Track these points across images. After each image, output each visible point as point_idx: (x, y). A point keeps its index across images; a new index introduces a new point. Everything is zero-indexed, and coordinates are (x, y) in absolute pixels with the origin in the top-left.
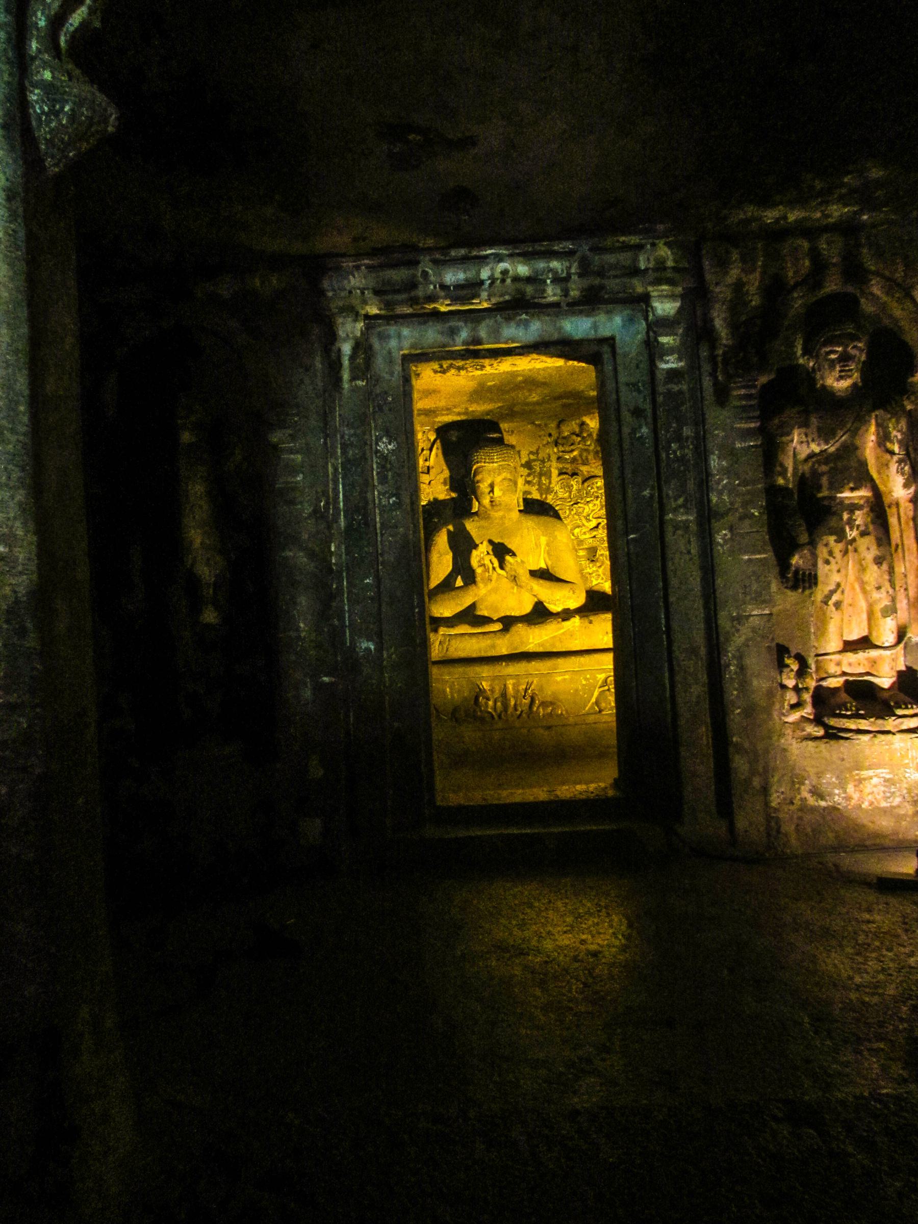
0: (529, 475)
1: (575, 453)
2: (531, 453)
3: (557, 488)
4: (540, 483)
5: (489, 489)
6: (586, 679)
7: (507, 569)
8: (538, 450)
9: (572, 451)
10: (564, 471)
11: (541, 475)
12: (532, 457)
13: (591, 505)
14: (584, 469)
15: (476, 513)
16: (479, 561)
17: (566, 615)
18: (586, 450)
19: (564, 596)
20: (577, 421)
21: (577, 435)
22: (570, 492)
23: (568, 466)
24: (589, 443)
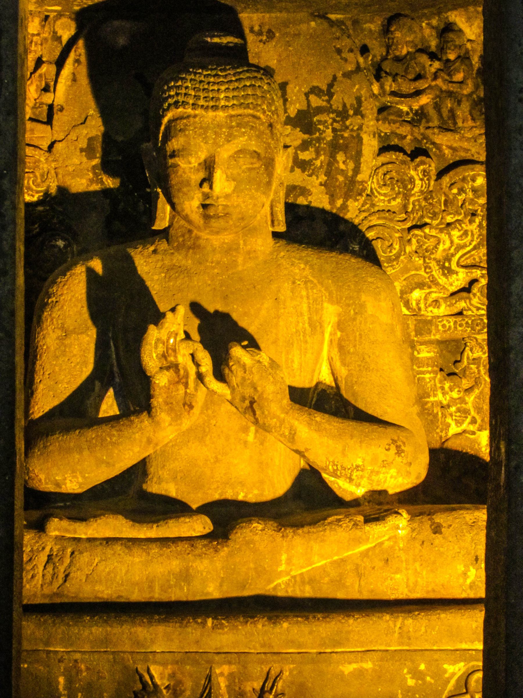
0: (304, 146)
1: (424, 100)
2: (315, 91)
3: (372, 184)
4: (330, 170)
5: (201, 175)
6: (417, 674)
7: (234, 381)
8: (330, 86)
9: (418, 93)
10: (395, 141)
11: (335, 147)
12: (316, 101)
13: (455, 233)
14: (444, 140)
15: (165, 234)
16: (164, 356)
17: (377, 506)
18: (450, 94)
19: (374, 460)
20: (434, 22)
21: (433, 56)
24: (459, 77)
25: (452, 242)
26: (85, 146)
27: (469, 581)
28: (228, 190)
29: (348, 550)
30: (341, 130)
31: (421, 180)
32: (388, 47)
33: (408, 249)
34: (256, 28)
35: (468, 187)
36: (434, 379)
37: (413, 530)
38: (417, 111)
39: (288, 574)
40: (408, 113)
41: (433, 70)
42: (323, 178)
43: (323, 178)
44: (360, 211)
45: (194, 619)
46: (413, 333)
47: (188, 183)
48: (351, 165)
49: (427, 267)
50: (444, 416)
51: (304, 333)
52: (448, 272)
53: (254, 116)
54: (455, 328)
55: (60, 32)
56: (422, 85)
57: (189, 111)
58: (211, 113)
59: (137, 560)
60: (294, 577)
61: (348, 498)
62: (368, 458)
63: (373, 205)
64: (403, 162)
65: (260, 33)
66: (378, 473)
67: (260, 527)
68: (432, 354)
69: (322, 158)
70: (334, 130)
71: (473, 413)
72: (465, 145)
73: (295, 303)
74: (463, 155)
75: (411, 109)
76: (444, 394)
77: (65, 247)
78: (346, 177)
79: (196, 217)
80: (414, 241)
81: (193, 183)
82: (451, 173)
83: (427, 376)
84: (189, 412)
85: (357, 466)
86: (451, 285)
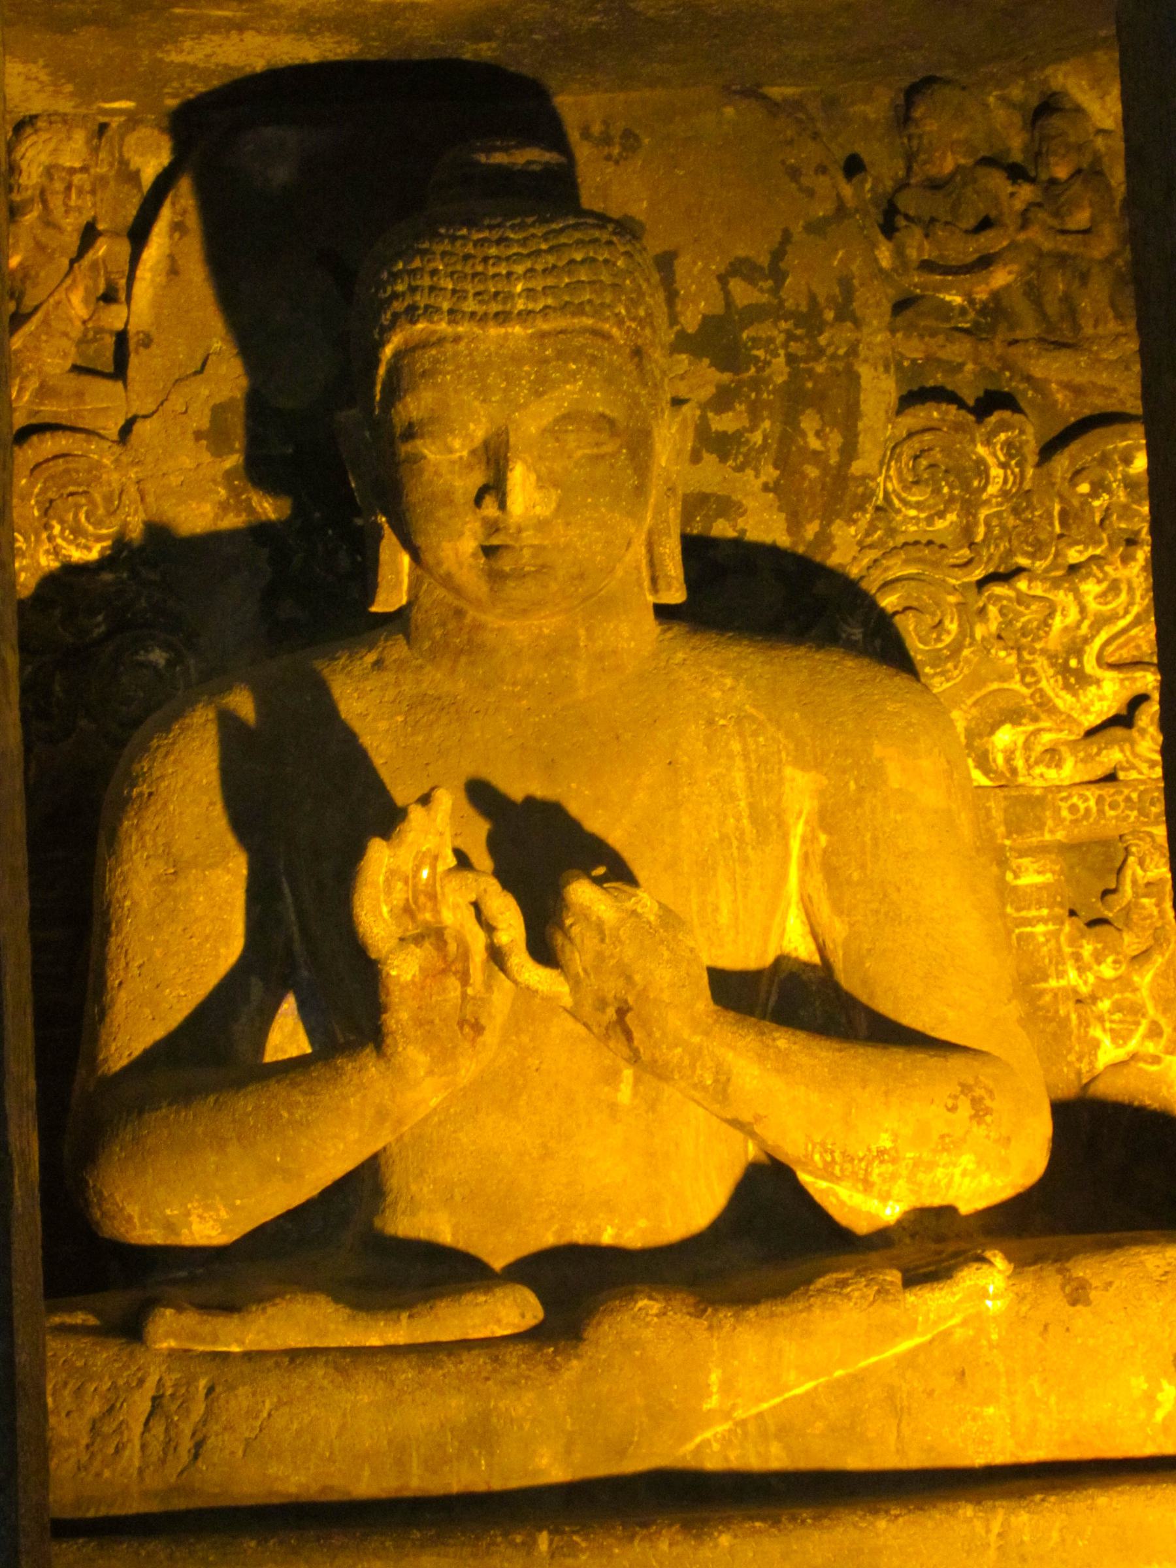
0: (722, 400)
1: (1001, 278)
2: (741, 268)
3: (887, 483)
5: (478, 478)
8: (778, 255)
9: (985, 262)
10: (938, 378)
11: (795, 399)
12: (743, 293)
13: (1090, 588)
14: (1051, 368)
15: (399, 620)
16: (408, 911)
17: (932, 1245)
18: (1062, 260)
19: (921, 1136)
20: (1016, 92)
21: (1016, 173)
22: (969, 507)
23: (957, 350)
24: (1081, 218)
25: (1083, 610)
26: (205, 424)
27: (1159, 1415)
28: (543, 511)
29: (868, 1356)
30: (806, 360)
31: (1004, 466)
32: (910, 158)
33: (979, 631)
34: (597, 129)
35: (1114, 477)
36: (1056, 935)
37: (1021, 1298)
38: (985, 305)
39: (727, 1415)
40: (963, 311)
41: (1019, 205)
42: (770, 473)
43: (770, 473)
44: (862, 547)
45: (505, 1534)
46: (1001, 830)
47: (448, 499)
48: (836, 439)
49: (1026, 671)
50: (1084, 1023)
51: (741, 840)
52: (1076, 680)
53: (595, 333)
54: (1101, 812)
55: (136, 162)
56: (991, 241)
57: (443, 327)
58: (494, 331)
59: (365, 1399)
60: (743, 1423)
61: (862, 1227)
62: (907, 1131)
63: (892, 532)
64: (958, 427)
65: (606, 140)
66: (931, 1166)
67: (655, 1307)
68: (1048, 877)
69: (767, 424)
70: (791, 359)
71: (1151, 1011)
72: (1104, 379)
73: (715, 771)
74: (1098, 403)
75: (972, 302)
76: (1081, 970)
77: (170, 664)
78: (825, 469)
79: (470, 577)
80: (993, 610)
81: (459, 497)
82: (1074, 447)
83: (1040, 928)
84: (473, 1041)
85: (882, 1152)
86: (1086, 711)
